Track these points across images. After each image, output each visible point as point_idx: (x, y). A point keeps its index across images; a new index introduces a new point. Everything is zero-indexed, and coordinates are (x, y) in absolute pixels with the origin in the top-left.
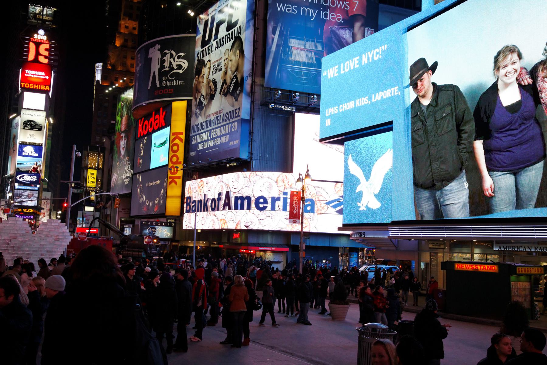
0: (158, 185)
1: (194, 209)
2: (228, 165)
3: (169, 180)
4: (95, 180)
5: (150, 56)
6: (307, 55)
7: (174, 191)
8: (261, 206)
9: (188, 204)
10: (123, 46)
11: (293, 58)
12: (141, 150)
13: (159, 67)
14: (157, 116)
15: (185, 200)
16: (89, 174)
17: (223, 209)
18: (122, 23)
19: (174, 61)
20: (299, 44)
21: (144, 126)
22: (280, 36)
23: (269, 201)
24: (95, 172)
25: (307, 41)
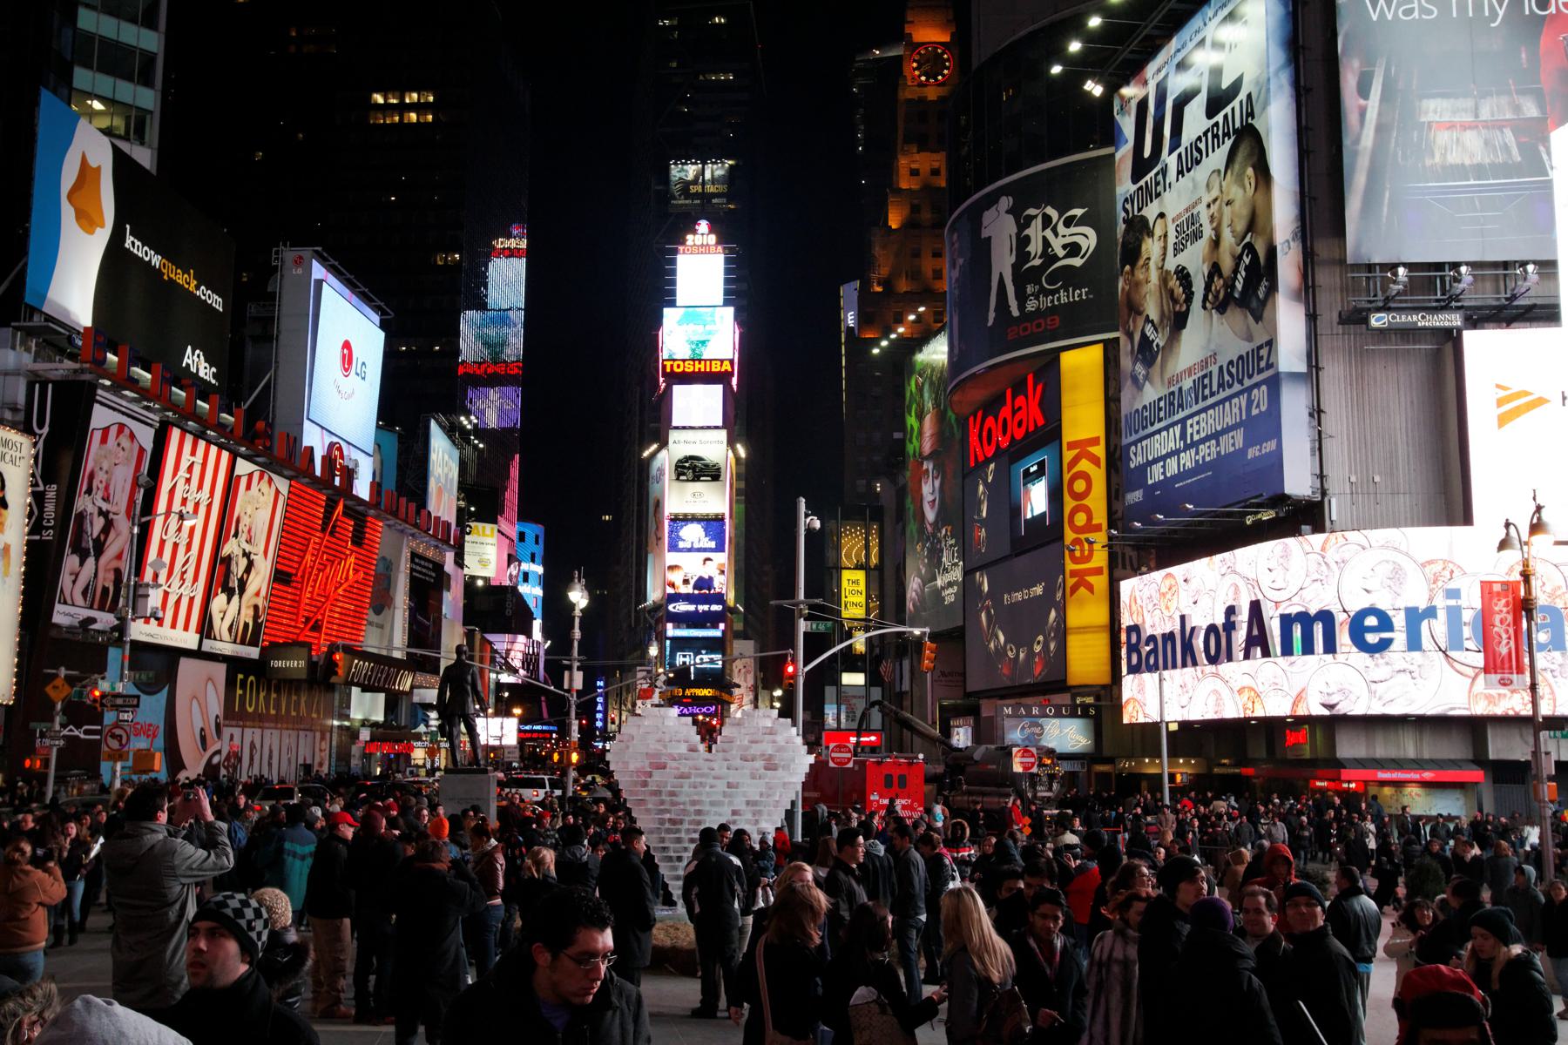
0: (1037, 598)
1: (1152, 661)
2: (1249, 520)
3: (1070, 582)
4: (862, 599)
5: (985, 234)
6: (1486, 143)
7: (1086, 613)
8: (1372, 638)
9: (1133, 648)
10: (910, 225)
11: (1437, 159)
12: (980, 502)
13: (1013, 259)
14: (1020, 400)
15: (1124, 637)
16: (845, 584)
17: (1247, 657)
18: (903, 162)
19: (1056, 235)
20: (1454, 112)
21: (985, 434)
22: (1386, 97)
23: (1399, 621)
24: (860, 575)
25: (1484, 95)
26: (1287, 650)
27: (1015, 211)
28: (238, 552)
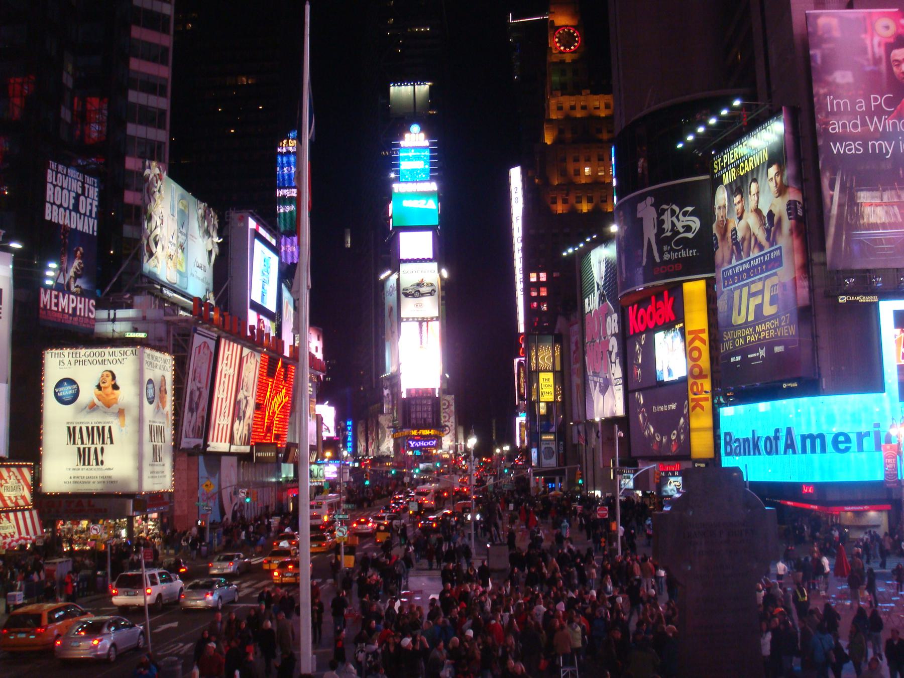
0: (672, 411)
3: (692, 404)
4: (552, 390)
5: (639, 215)
6: (887, 212)
7: (700, 421)
8: (842, 446)
10: (557, 142)
11: (865, 220)
12: (637, 355)
13: (655, 231)
14: (660, 303)
16: (541, 381)
17: (785, 453)
18: (553, 103)
20: (873, 198)
22: (842, 190)
23: (854, 438)
24: (550, 376)
25: (884, 190)
26: (804, 451)
27: (656, 205)
28: (243, 397)
